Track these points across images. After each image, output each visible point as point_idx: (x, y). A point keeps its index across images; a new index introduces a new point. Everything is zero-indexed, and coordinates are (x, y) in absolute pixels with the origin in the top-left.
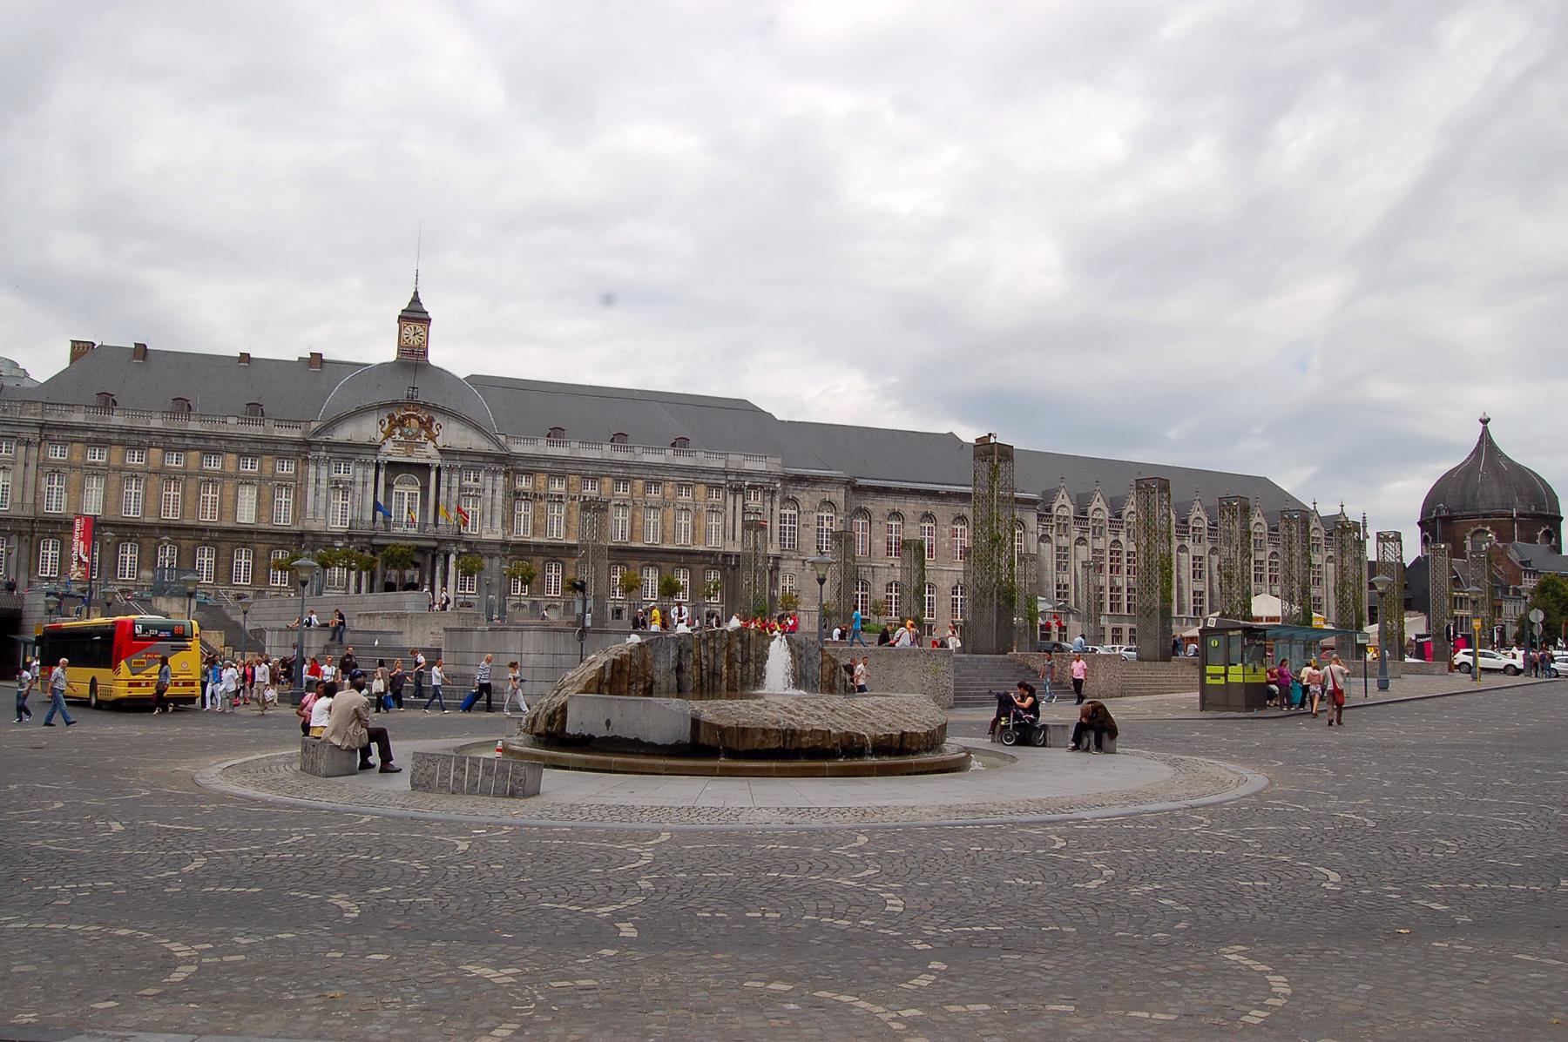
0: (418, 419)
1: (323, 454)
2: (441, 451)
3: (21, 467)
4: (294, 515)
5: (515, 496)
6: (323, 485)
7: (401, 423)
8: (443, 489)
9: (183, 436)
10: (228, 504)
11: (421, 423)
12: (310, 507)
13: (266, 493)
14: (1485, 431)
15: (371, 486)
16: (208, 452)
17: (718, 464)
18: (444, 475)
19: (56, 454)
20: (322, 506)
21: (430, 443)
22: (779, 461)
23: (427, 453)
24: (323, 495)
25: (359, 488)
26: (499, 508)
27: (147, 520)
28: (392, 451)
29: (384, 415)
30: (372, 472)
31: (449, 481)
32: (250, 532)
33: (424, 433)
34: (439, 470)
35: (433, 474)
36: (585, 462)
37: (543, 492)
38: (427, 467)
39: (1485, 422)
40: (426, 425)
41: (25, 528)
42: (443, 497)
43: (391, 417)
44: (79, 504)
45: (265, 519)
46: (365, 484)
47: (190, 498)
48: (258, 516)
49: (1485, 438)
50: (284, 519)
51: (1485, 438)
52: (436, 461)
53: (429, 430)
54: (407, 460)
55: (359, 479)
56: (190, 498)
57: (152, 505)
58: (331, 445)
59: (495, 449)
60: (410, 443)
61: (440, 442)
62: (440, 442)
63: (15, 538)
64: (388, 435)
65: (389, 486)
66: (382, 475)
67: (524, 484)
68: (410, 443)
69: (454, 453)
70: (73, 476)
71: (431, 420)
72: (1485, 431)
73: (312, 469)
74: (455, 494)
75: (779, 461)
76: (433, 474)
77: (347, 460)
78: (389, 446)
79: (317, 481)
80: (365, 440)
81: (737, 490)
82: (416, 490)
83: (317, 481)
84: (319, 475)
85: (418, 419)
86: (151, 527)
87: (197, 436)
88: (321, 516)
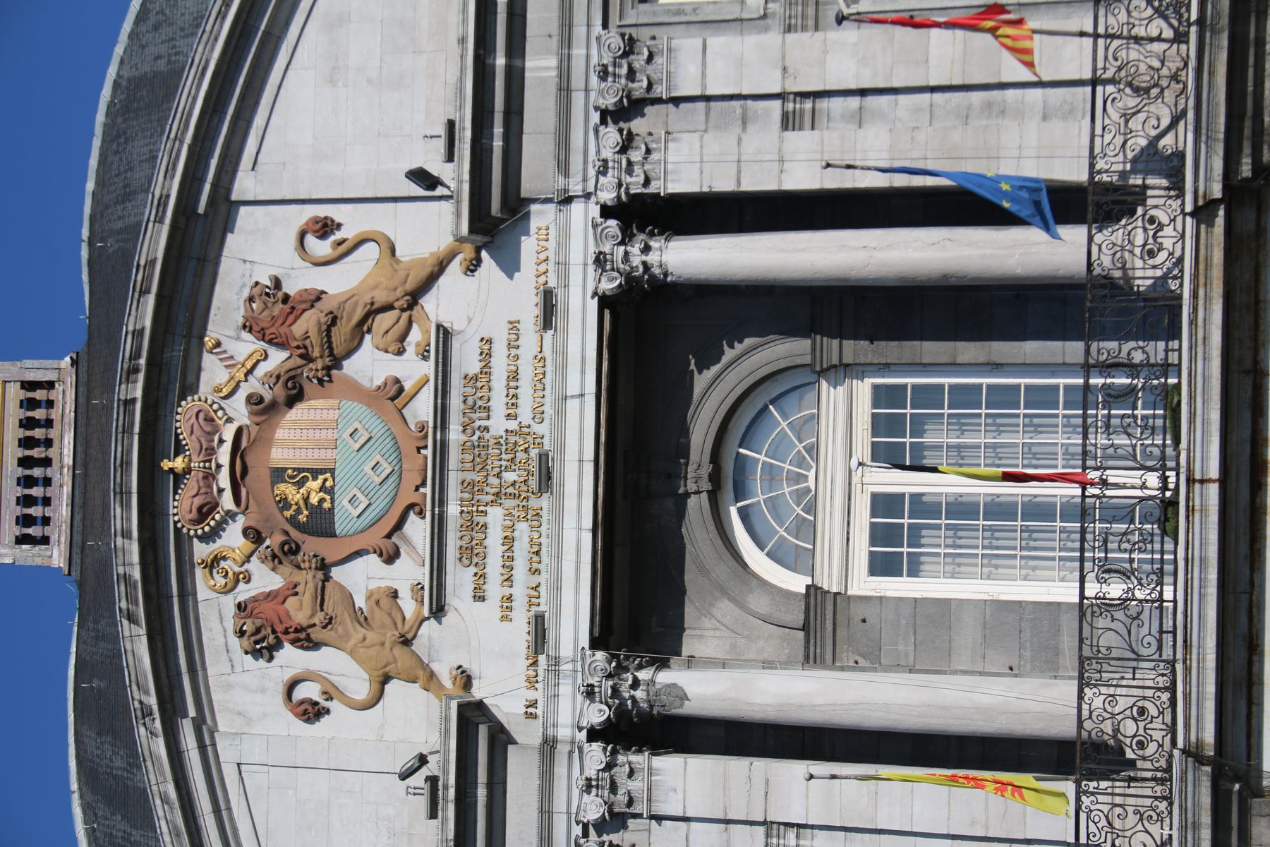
0: (264, 409)
7: (302, 536)
18: (690, 162)
21: (450, 301)
23: (528, 339)
30: (681, 779)
33: (369, 365)
34: (645, 214)
40: (313, 348)
61: (432, 228)
65: (821, 627)
69: (494, 102)
71: (274, 310)
78: (484, 644)
82: (845, 409)
85: (264, 409)
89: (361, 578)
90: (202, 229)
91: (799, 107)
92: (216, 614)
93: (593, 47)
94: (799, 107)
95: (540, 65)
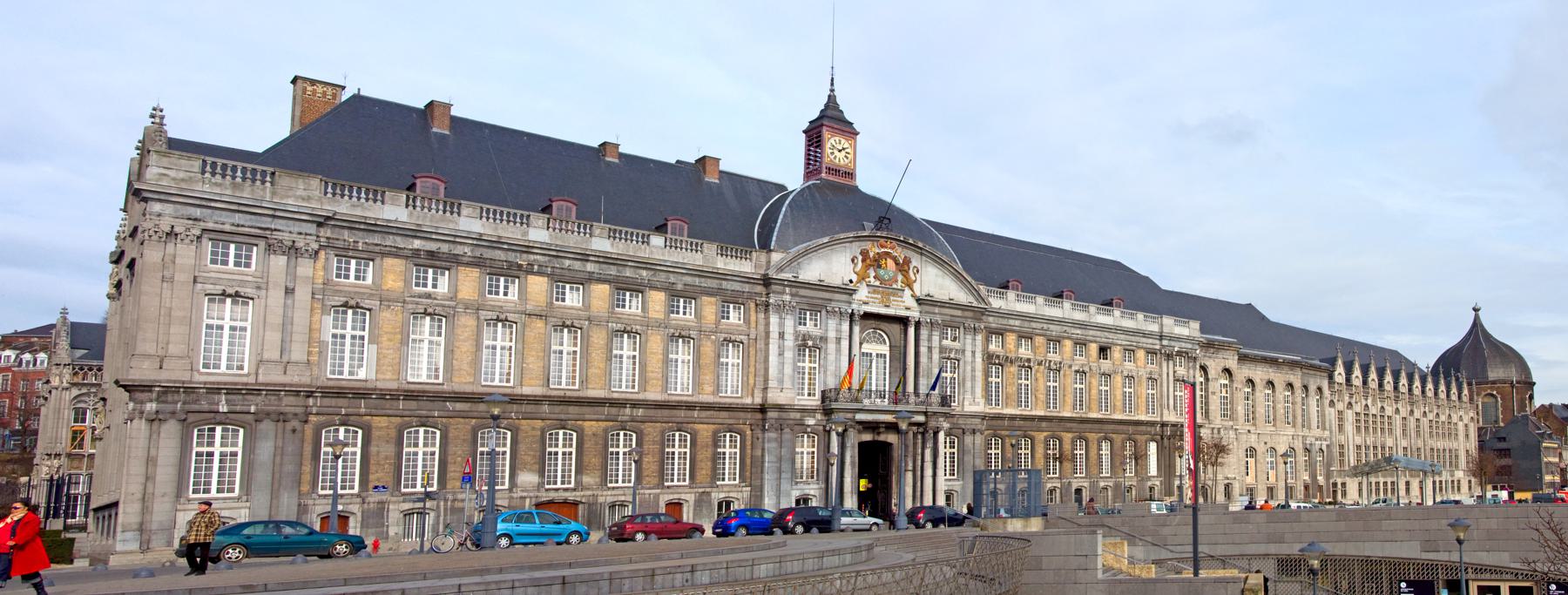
0: (895, 259)
1: (788, 298)
2: (919, 301)
3: (276, 296)
4: (745, 383)
5: (989, 358)
6: (790, 342)
7: (877, 263)
8: (923, 350)
9: (584, 257)
10: (655, 364)
11: (897, 264)
12: (773, 372)
13: (708, 349)
14: (1477, 318)
15: (845, 343)
16: (623, 287)
17: (1154, 328)
18: (924, 333)
19: (362, 278)
20: (788, 370)
21: (908, 292)
22: (1195, 325)
24: (789, 355)
25: (832, 346)
26: (979, 374)
27: (527, 390)
28: (865, 299)
29: (856, 249)
30: (846, 326)
31: (930, 340)
32: (690, 406)
33: (900, 277)
34: (918, 324)
35: (911, 331)
36: (1051, 321)
37: (1012, 355)
38: (903, 321)
39: (1476, 310)
40: (903, 267)
41: (289, 404)
42: (923, 360)
43: (865, 254)
44: (401, 364)
45: (708, 389)
46: (838, 340)
47: (597, 356)
48: (697, 383)
49: (1476, 324)
50: (733, 386)
51: (1476, 324)
52: (914, 314)
53: (905, 273)
54: (883, 311)
55: (832, 334)
56: (597, 356)
57: (534, 364)
58: (796, 284)
59: (975, 304)
60: (886, 289)
62: (916, 287)
63: (267, 426)
64: (862, 277)
66: (857, 329)
67: (993, 347)
68: (886, 289)
70: (386, 314)
71: (907, 261)
72: (1477, 318)
73: (774, 319)
74: (936, 356)
75: (1195, 325)
76: (911, 331)
77: (816, 308)
78: (863, 293)
79: (782, 335)
80: (836, 281)
81: (1169, 357)
82: (885, 349)
83: (782, 335)
84: (784, 327)
85: (895, 259)
86: (536, 400)
87: (606, 259)
88: (787, 384)
89: (872, 274)
90: (921, 251)
91: (930, 349)
92: (867, 245)
93: (939, 319)
94: (930, 349)
95: (937, 310)
